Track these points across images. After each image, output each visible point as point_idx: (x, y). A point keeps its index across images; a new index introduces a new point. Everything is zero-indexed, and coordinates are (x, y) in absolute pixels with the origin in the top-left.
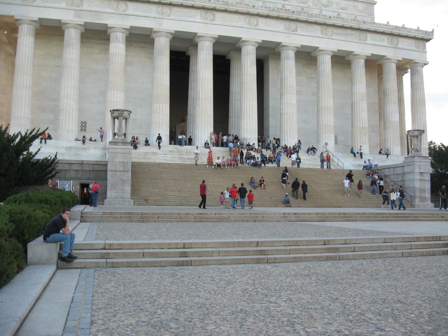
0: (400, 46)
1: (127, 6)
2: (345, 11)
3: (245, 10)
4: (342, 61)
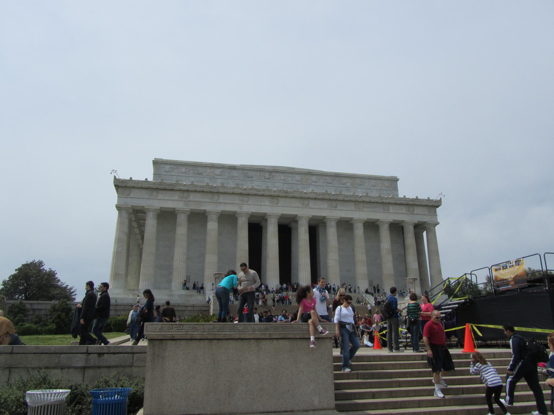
0: (415, 212)
1: (219, 197)
2: (375, 188)
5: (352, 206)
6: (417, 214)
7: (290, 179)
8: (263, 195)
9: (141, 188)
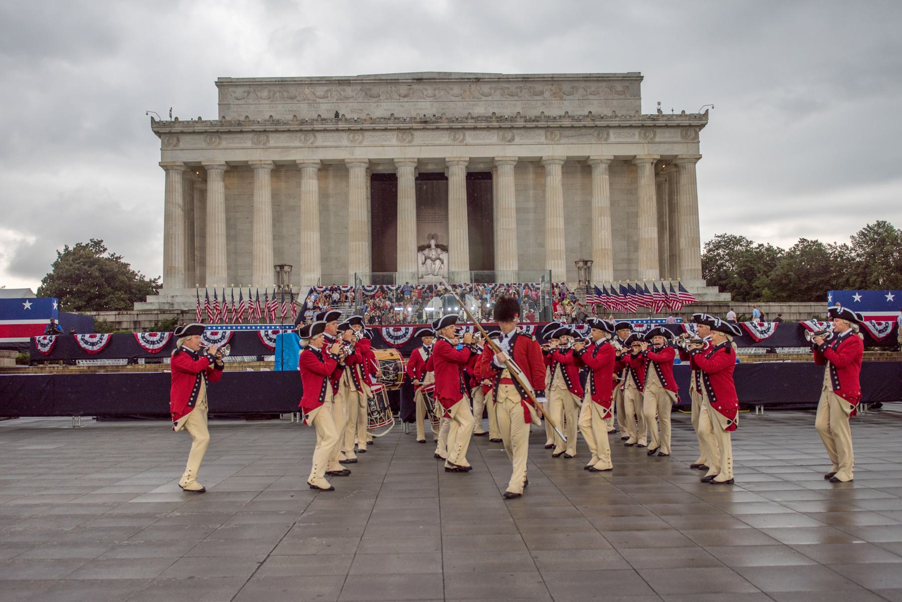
0: (657, 139)
1: (315, 137)
3: (445, 125)
4: (580, 168)
5: (541, 137)
6: (660, 143)
7: (442, 93)
8: (386, 130)
9: (194, 133)
